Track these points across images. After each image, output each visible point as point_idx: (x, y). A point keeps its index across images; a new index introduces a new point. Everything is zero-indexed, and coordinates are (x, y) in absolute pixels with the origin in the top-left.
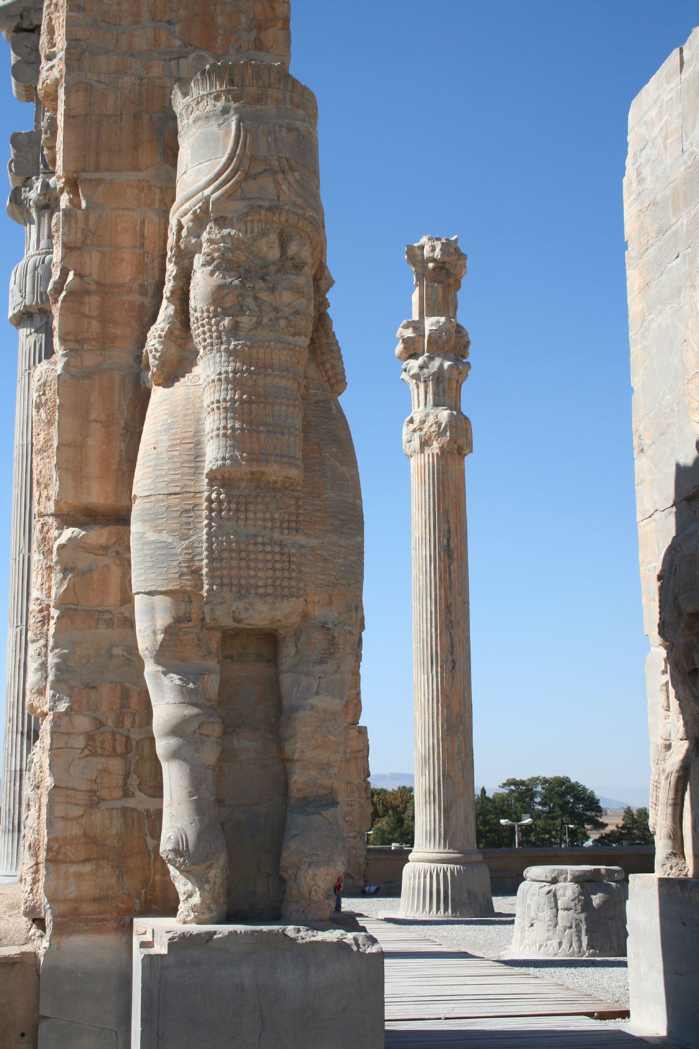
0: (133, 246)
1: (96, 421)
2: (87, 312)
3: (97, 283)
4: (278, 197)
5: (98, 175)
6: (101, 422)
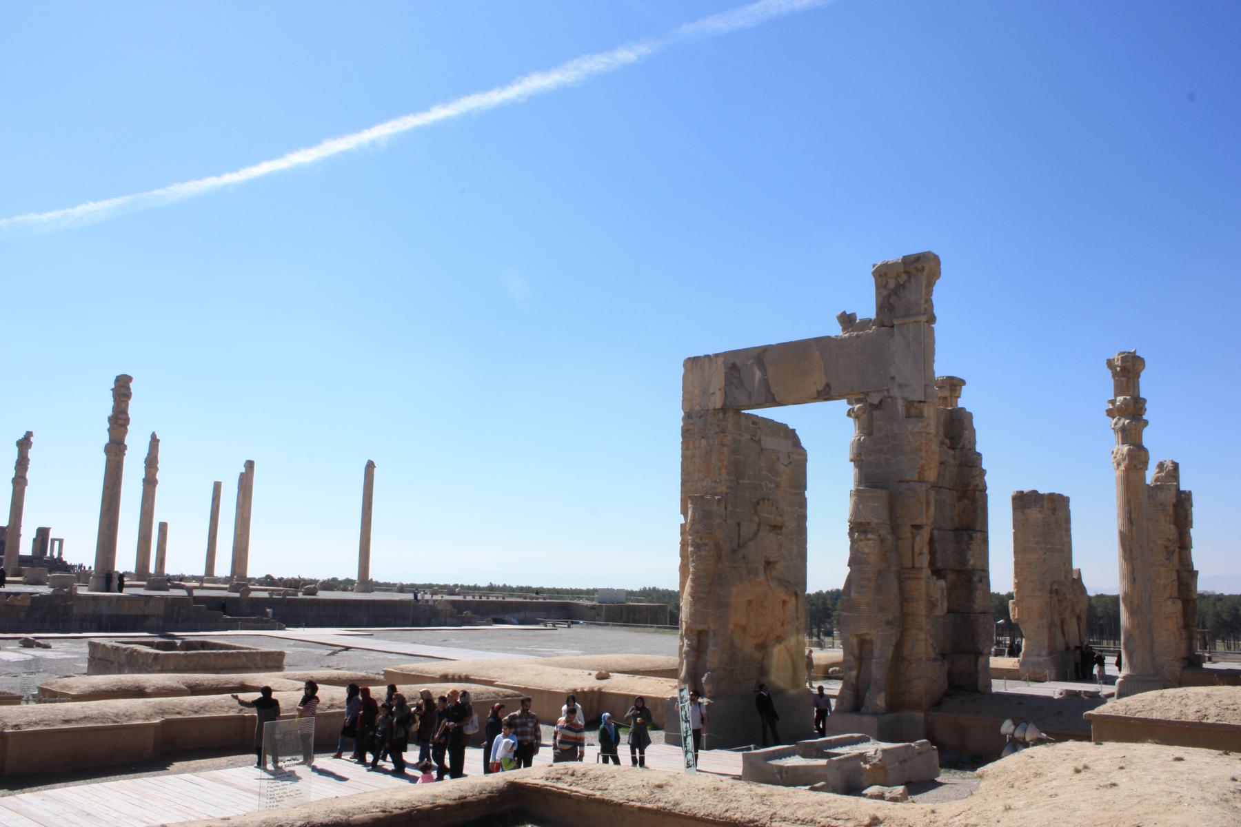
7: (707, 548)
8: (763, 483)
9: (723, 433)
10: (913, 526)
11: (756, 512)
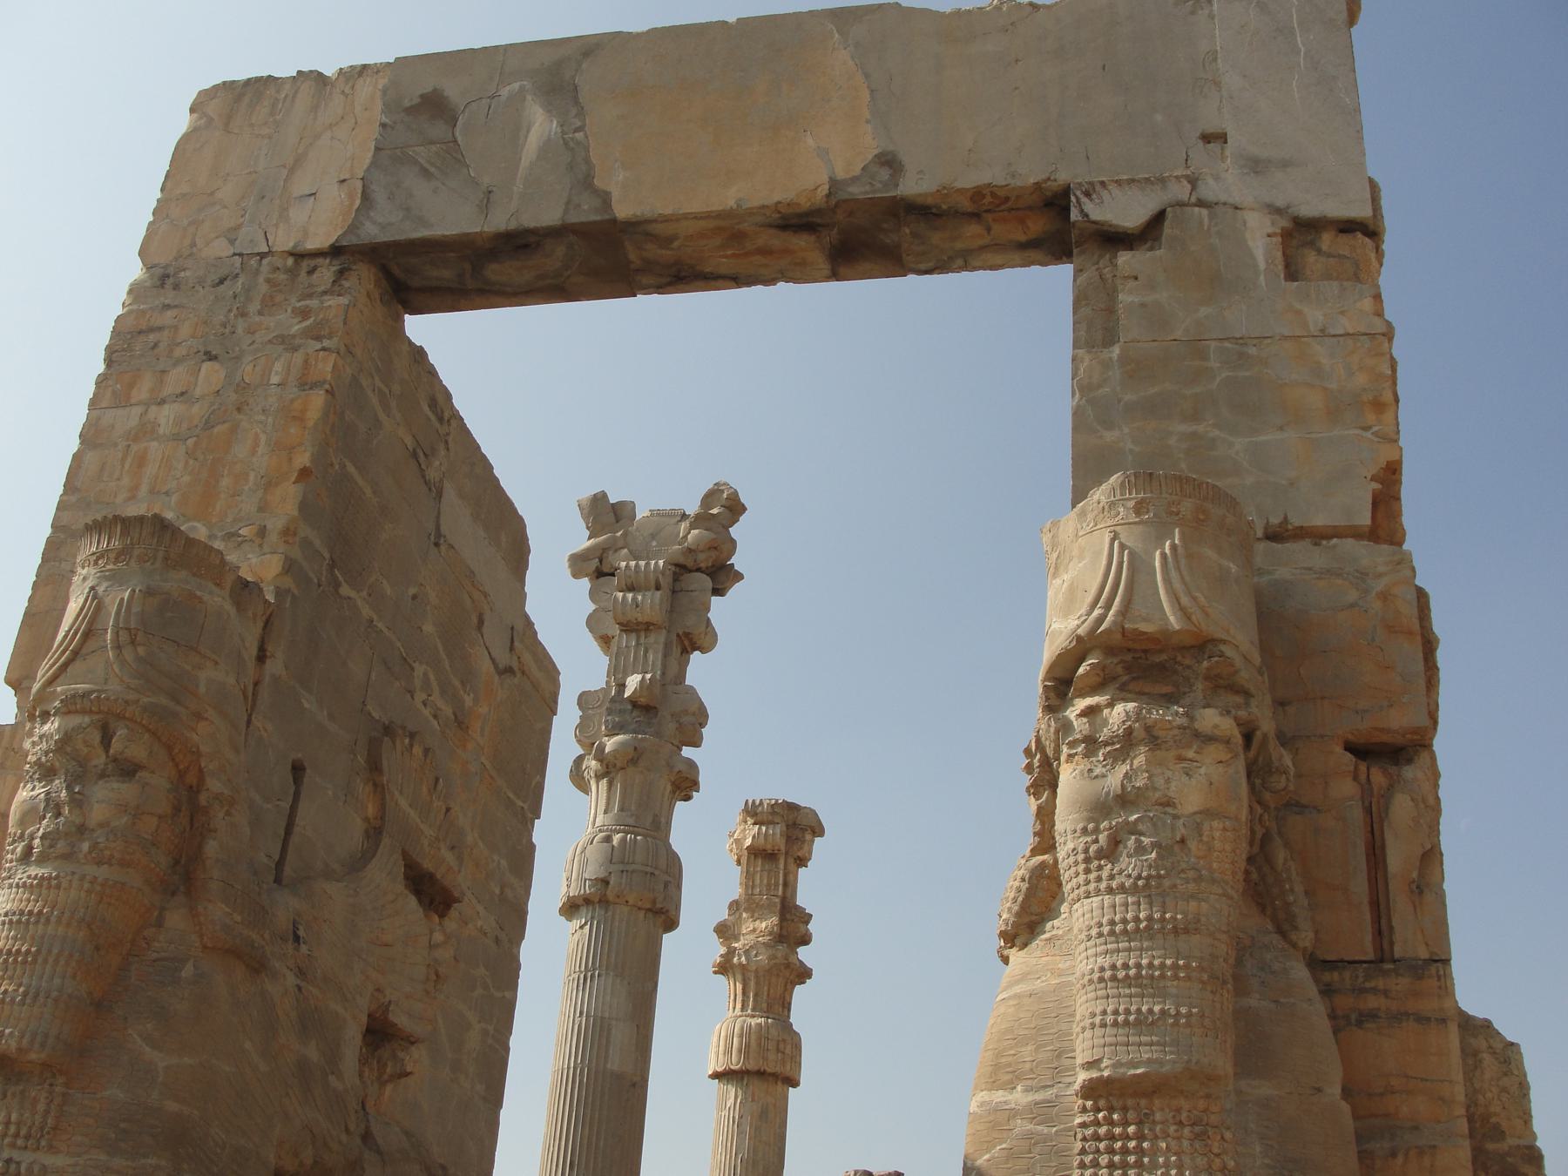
7: (126, 790)
8: (420, 669)
9: (318, 338)
10: (1362, 751)
11: (374, 766)
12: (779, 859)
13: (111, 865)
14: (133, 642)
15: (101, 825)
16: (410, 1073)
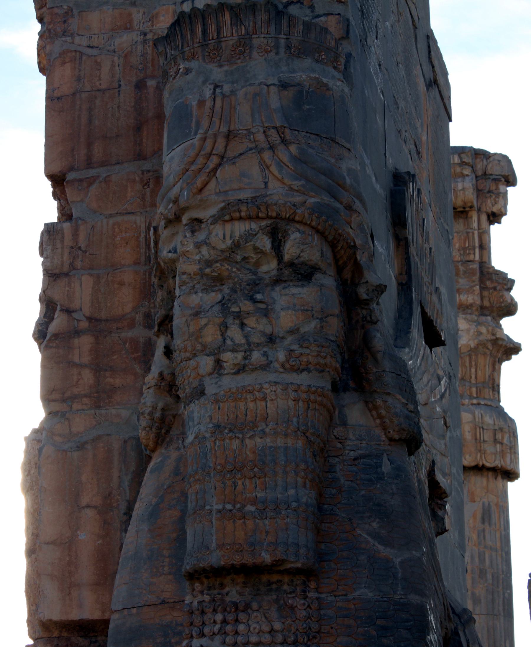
0: (137, 263)
1: (88, 506)
2: (76, 359)
3: (89, 319)
4: (266, 184)
5: (92, 172)
6: (95, 507)
12: (471, 217)
13: (309, 371)
14: (284, 141)
15: (291, 332)
16: (448, 530)
